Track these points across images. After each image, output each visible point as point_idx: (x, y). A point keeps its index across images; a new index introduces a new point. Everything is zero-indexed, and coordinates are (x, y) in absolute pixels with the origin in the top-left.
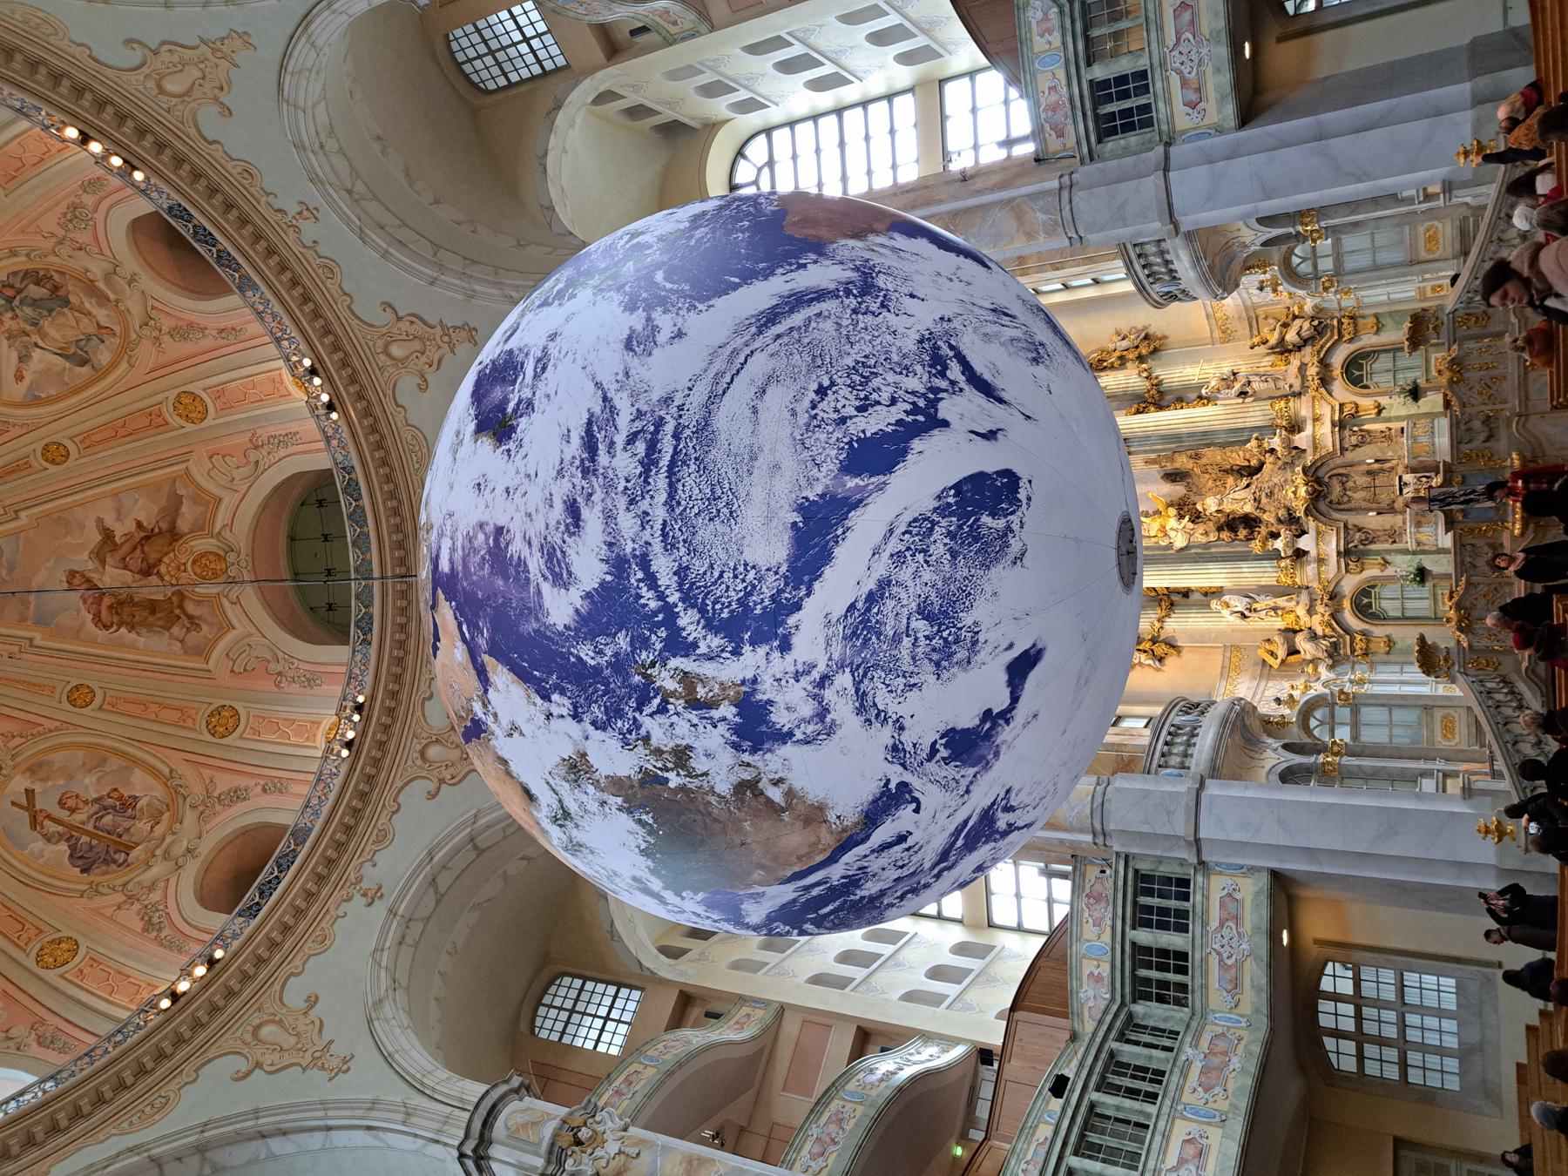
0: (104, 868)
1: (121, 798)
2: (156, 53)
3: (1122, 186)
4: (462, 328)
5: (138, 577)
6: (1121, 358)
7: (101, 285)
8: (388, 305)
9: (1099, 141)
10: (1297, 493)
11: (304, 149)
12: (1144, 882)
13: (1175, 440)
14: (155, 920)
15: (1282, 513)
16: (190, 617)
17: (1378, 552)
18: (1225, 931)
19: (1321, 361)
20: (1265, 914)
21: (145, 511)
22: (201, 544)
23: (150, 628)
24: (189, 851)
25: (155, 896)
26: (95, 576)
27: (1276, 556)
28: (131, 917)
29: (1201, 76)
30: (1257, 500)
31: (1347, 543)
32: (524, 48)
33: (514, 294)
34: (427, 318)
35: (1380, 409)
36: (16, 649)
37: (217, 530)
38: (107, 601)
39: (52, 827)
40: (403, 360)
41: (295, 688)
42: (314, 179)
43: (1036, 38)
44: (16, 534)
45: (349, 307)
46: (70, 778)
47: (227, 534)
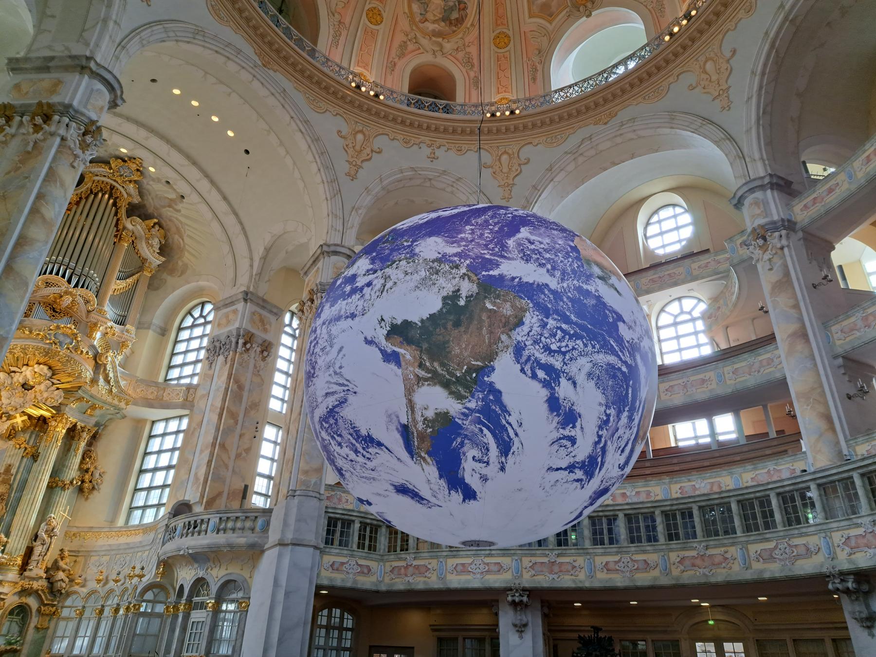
2: (520, 165)
7: (440, 40)
9: (329, 518)
33: (360, 212)
42: (444, 172)
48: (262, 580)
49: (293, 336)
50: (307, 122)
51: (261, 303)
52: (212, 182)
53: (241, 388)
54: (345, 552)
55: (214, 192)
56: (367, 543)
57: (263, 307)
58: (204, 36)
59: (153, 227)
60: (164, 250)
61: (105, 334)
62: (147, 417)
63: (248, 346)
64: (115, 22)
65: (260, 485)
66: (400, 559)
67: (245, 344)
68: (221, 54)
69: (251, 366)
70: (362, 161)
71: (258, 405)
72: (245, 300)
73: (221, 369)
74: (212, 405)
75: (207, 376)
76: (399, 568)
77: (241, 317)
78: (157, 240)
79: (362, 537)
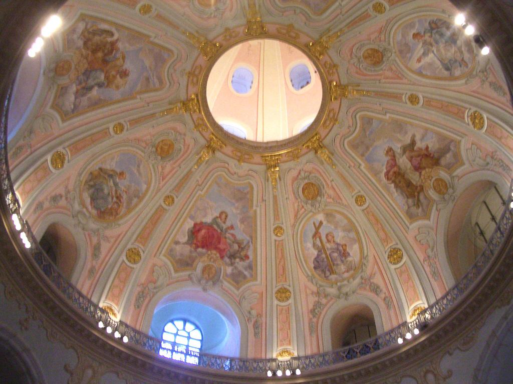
0: (320, 273)
1: (345, 250)
5: (412, 168)
14: (316, 311)
16: (419, 200)
21: (432, 144)
22: (443, 174)
23: (402, 192)
24: (347, 294)
25: (324, 301)
26: (397, 156)
28: (312, 300)
36: (352, 165)
37: (454, 174)
38: (395, 169)
39: (318, 243)
41: (428, 269)
44: (381, 121)
46: (336, 228)
47: (456, 180)
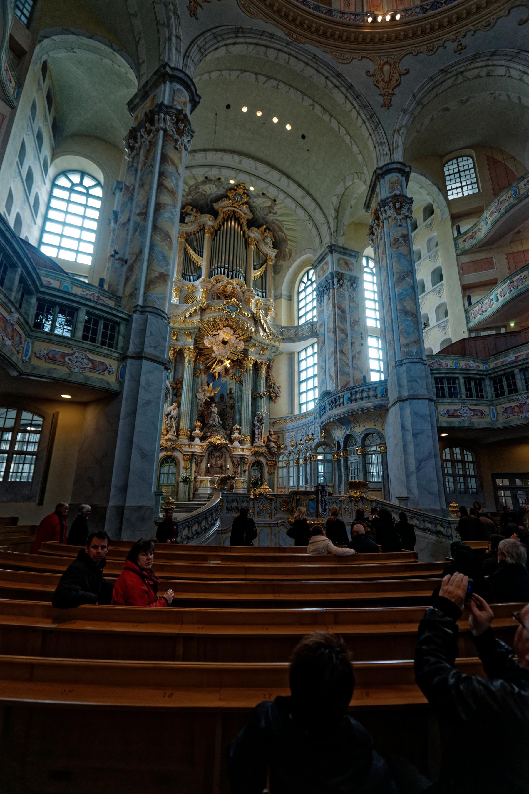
3: (425, 383)
4: (390, 103)
6: (270, 386)
8: (408, 72)
10: (218, 439)
11: (491, 56)
12: (112, 326)
13: (240, 399)
15: (209, 434)
17: (191, 466)
18: (86, 361)
19: (263, 453)
20: (98, 384)
27: (192, 429)
29: (457, 416)
30: (214, 426)
31: (197, 455)
32: (459, 185)
33: (401, 132)
34: (397, 88)
35: (244, 471)
40: (382, 69)
43: (464, 363)
45: (411, 53)
48: (391, 428)
49: (372, 273)
50: (338, 75)
51: (342, 251)
52: (289, 177)
53: (343, 312)
54: (457, 401)
55: (292, 184)
56: (474, 393)
57: (345, 254)
58: (243, 33)
59: (265, 231)
60: (275, 246)
61: (257, 305)
62: (294, 350)
63: (341, 282)
64: (176, 36)
65: (374, 365)
66: (511, 401)
67: (338, 282)
68: (261, 45)
69: (347, 296)
70: (393, 89)
71: (358, 322)
72: (331, 252)
73: (327, 303)
74: (328, 328)
75: (321, 312)
76: (513, 408)
77: (331, 264)
78: (269, 239)
79: (468, 389)
